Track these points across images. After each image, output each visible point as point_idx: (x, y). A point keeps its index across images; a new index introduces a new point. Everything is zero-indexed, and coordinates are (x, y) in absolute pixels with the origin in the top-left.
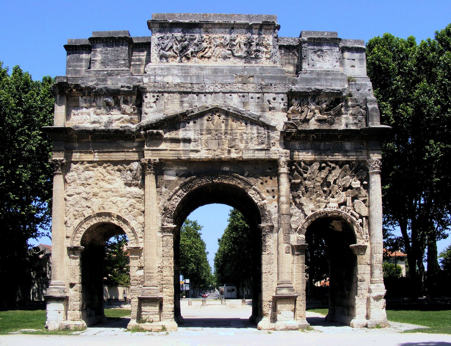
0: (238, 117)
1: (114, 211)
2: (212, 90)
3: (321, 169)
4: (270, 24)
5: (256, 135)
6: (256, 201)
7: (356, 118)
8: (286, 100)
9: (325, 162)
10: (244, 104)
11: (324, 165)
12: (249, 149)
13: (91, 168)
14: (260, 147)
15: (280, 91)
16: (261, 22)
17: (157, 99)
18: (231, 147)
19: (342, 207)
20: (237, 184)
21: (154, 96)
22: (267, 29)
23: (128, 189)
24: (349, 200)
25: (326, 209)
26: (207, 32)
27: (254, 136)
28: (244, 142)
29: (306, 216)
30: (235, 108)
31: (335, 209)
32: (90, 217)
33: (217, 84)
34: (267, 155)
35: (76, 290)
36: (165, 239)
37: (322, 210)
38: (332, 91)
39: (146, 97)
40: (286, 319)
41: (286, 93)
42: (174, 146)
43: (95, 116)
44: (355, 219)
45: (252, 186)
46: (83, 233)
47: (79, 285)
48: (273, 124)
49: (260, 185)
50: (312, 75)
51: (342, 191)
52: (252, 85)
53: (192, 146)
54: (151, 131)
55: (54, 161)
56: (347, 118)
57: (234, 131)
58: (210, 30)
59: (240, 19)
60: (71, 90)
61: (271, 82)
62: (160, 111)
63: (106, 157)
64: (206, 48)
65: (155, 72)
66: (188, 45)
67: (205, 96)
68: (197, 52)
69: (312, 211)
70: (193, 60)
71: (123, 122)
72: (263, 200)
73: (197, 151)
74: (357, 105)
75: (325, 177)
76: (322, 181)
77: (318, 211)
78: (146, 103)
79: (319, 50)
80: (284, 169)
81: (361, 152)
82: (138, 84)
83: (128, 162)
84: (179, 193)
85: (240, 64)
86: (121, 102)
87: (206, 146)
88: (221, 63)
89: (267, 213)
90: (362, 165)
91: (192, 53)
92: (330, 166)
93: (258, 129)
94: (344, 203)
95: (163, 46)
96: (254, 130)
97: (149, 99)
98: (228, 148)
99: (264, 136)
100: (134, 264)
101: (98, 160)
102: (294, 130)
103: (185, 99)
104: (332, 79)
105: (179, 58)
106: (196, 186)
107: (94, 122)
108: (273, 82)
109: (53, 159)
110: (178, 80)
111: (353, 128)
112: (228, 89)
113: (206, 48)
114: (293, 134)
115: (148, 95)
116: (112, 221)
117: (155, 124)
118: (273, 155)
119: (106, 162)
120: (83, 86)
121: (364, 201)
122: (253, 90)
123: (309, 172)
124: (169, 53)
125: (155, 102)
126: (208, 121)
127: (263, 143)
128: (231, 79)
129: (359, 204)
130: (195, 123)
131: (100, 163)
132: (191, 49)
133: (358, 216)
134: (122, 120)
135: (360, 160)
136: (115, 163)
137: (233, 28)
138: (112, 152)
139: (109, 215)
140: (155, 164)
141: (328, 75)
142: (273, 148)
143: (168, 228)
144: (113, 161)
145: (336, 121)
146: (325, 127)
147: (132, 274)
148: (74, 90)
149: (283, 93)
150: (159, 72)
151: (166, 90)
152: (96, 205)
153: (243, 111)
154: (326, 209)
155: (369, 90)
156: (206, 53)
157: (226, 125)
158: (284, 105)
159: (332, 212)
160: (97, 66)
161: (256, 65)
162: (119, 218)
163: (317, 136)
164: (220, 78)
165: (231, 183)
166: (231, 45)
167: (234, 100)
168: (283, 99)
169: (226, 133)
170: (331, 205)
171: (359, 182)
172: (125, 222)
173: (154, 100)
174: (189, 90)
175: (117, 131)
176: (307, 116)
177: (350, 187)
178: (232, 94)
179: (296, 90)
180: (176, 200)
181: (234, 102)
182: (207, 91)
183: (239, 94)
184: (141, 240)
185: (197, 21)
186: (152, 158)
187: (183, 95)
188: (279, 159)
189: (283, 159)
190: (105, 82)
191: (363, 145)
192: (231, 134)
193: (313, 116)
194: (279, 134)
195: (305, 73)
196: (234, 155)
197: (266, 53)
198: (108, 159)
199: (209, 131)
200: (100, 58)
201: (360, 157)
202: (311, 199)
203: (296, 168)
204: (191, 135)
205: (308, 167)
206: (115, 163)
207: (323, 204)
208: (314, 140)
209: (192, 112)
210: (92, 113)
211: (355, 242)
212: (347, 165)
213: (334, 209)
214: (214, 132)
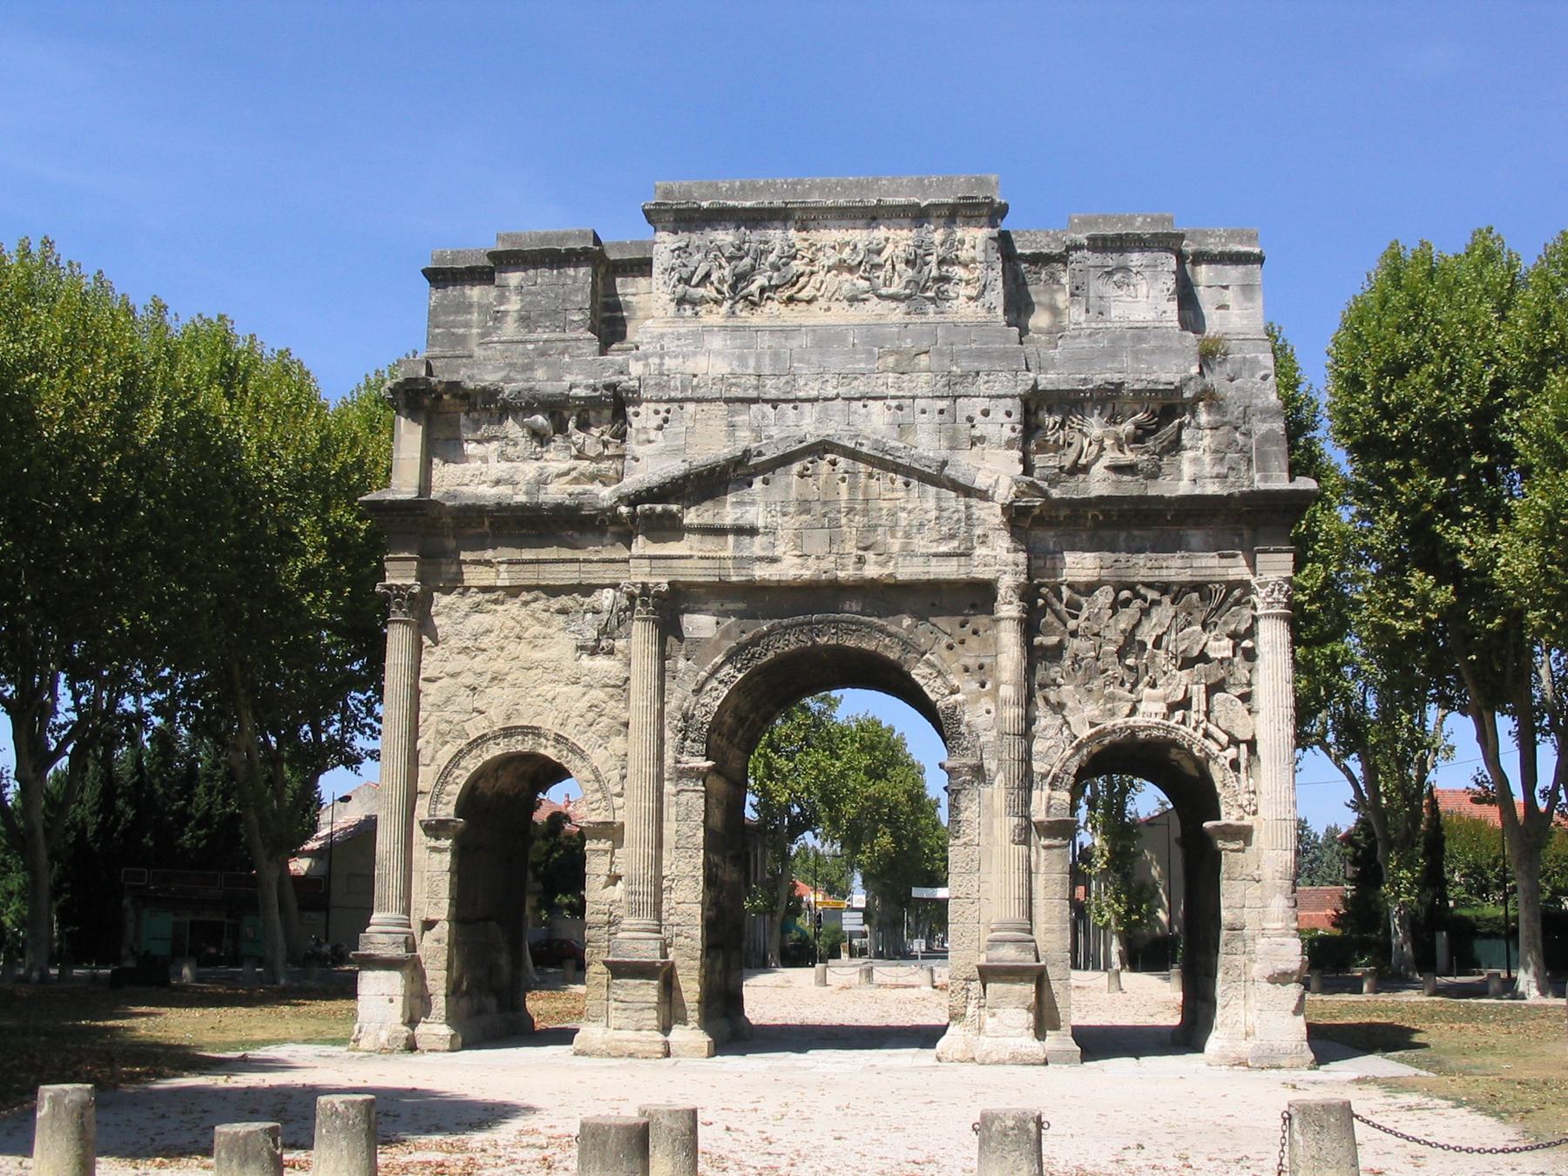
0: (883, 463)
1: (548, 723)
2: (813, 394)
3: (1117, 606)
4: (978, 204)
5: (933, 514)
6: (933, 697)
7: (1222, 459)
8: (1016, 416)
9: (1131, 587)
10: (903, 428)
11: (1125, 594)
12: (912, 554)
13: (494, 607)
14: (943, 548)
15: (1002, 393)
16: (950, 201)
17: (666, 420)
18: (865, 549)
19: (1179, 714)
20: (880, 650)
21: (657, 412)
22: (971, 217)
23: (586, 661)
25: (1131, 721)
26: (803, 227)
27: (928, 516)
28: (900, 534)
30: (877, 441)
31: (1158, 719)
32: (482, 740)
33: (827, 377)
34: (962, 570)
35: (438, 941)
36: (684, 798)
37: (1120, 721)
38: (1150, 386)
39: (637, 414)
40: (1011, 1032)
41: (1020, 396)
42: (710, 545)
43: (505, 465)
44: (1214, 748)
45: (924, 654)
46: (462, 782)
47: (446, 926)
48: (981, 482)
49: (946, 653)
50: (1096, 342)
52: (924, 377)
53: (757, 546)
54: (647, 506)
55: (389, 587)
56: (1196, 461)
57: (872, 504)
58: (812, 224)
59: (897, 193)
60: (439, 397)
61: (977, 365)
62: (676, 451)
63: (528, 575)
64: (802, 275)
65: (662, 348)
66: (753, 268)
67: (795, 408)
68: (777, 287)
69: (1092, 725)
70: (766, 310)
71: (576, 481)
72: (952, 693)
73: (774, 560)
74: (1224, 424)
76: (1121, 640)
77: (1109, 724)
78: (638, 430)
79: (1118, 269)
81: (1234, 556)
82: (615, 379)
83: (588, 590)
84: (721, 675)
85: (896, 314)
86: (571, 425)
87: (796, 547)
88: (841, 315)
89: (963, 729)
90: (1237, 593)
91: (763, 290)
92: (1145, 600)
93: (939, 499)
94: (1185, 704)
95: (685, 273)
96: (927, 500)
97: (643, 418)
98: (855, 552)
99: (956, 516)
100: (596, 867)
101: (507, 583)
102: (1038, 502)
103: (738, 419)
104: (1153, 352)
105: (727, 304)
106: (771, 655)
107: (497, 482)
108: (985, 366)
109: (388, 582)
110: (721, 367)
111: (1212, 489)
112: (859, 387)
113: (802, 275)
114: (1037, 511)
115: (642, 409)
116: (542, 751)
117: (659, 487)
118: (981, 569)
119: (529, 589)
120: (471, 385)
121: (1246, 698)
122: (926, 391)
123: (1084, 614)
124: (701, 291)
125: (660, 428)
126: (802, 476)
127: (952, 537)
128: (867, 361)
130: (766, 482)
131: (513, 591)
132: (761, 280)
133: (1224, 739)
134: (574, 474)
135: (1231, 578)
136: (553, 591)
137: (874, 219)
138: (545, 562)
139: (535, 732)
140: (658, 595)
141: (1140, 339)
142: (980, 551)
143: (692, 769)
144: (547, 586)
145: (1166, 469)
146: (1131, 487)
147: (590, 895)
148: (446, 397)
149: (1013, 397)
150: (671, 345)
151: (689, 394)
152: (496, 707)
153: (898, 449)
154: (1131, 721)
155: (1265, 378)
156: (800, 290)
157: (852, 488)
158: (1013, 430)
159: (1149, 728)
160: (510, 329)
161: (938, 318)
162: (559, 739)
163: (1107, 514)
164: (834, 360)
165: (864, 645)
166: (868, 263)
167: (874, 417)
168: (1009, 414)
169: (850, 510)
170: (1142, 707)
171: (1227, 643)
172: (574, 749)
173: (658, 420)
174: (752, 394)
175: (558, 508)
176: (1079, 457)
177: (1203, 657)
178: (870, 402)
179: (1050, 387)
180: (714, 694)
181: (875, 424)
182: (801, 394)
183: (888, 402)
184: (618, 801)
185: (778, 203)
186: (652, 581)
187: (738, 406)
188: (996, 580)
190: (528, 374)
191: (1241, 535)
192: (866, 512)
193: (1098, 456)
194: (999, 511)
195: (1074, 337)
196: (872, 571)
197: (968, 283)
198: (534, 582)
199: (804, 506)
200: (517, 307)
202: (1090, 691)
203: (1048, 604)
204: (755, 515)
205: (1083, 600)
206: (553, 591)
207: (1122, 704)
208: (1098, 525)
209: (760, 454)
210: (493, 458)
211: (1216, 816)
212: (1195, 596)
214: (818, 509)
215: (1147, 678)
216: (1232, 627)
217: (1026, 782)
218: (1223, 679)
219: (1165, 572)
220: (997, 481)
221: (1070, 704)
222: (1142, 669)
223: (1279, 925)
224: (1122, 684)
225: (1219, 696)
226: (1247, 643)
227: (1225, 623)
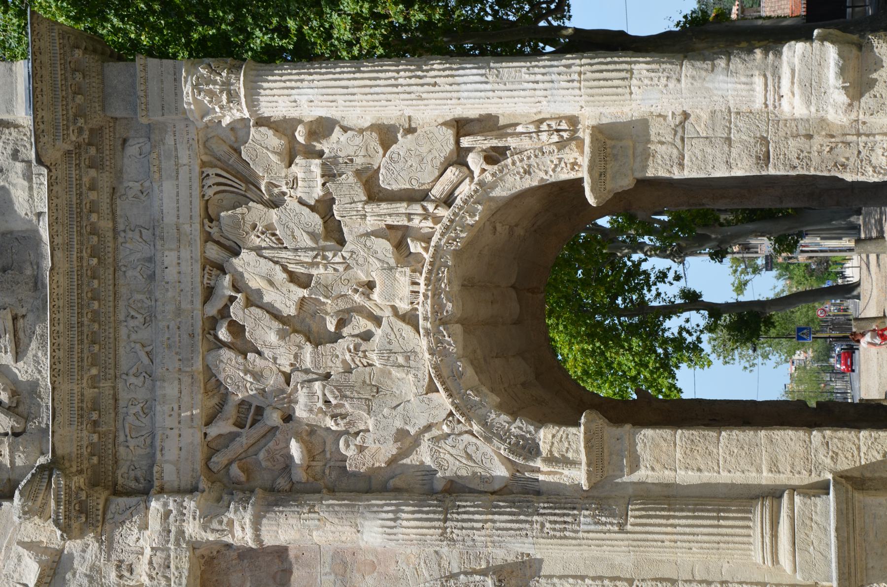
19: (415, 247)
24: (377, 216)
29: (451, 414)
31: (422, 281)
51: (342, 242)
69: (432, 388)
75: (276, 325)
76: (299, 338)
80: (241, 529)
129: (398, 167)
133: (452, 174)
159: (436, 294)
171: (298, 169)
177: (324, 207)
188: (194, 546)
189: (192, 529)
194: (73, 546)
201: (184, 159)
211: (581, 180)
213: (422, 288)
215: (357, 298)
216: (274, 158)
217: (522, 495)
218: (358, 173)
219: (185, 267)
220: (30, 546)
221: (399, 424)
222: (342, 305)
223: (759, 81)
224: (367, 336)
225: (386, 182)
226: (300, 136)
227: (268, 169)
